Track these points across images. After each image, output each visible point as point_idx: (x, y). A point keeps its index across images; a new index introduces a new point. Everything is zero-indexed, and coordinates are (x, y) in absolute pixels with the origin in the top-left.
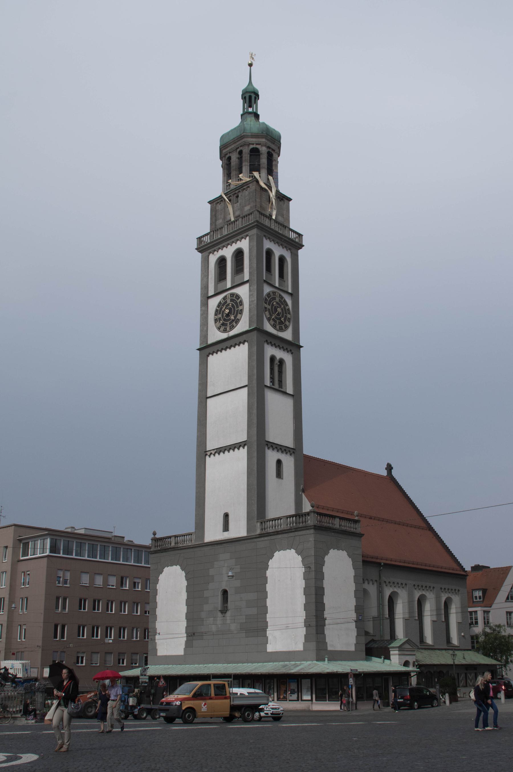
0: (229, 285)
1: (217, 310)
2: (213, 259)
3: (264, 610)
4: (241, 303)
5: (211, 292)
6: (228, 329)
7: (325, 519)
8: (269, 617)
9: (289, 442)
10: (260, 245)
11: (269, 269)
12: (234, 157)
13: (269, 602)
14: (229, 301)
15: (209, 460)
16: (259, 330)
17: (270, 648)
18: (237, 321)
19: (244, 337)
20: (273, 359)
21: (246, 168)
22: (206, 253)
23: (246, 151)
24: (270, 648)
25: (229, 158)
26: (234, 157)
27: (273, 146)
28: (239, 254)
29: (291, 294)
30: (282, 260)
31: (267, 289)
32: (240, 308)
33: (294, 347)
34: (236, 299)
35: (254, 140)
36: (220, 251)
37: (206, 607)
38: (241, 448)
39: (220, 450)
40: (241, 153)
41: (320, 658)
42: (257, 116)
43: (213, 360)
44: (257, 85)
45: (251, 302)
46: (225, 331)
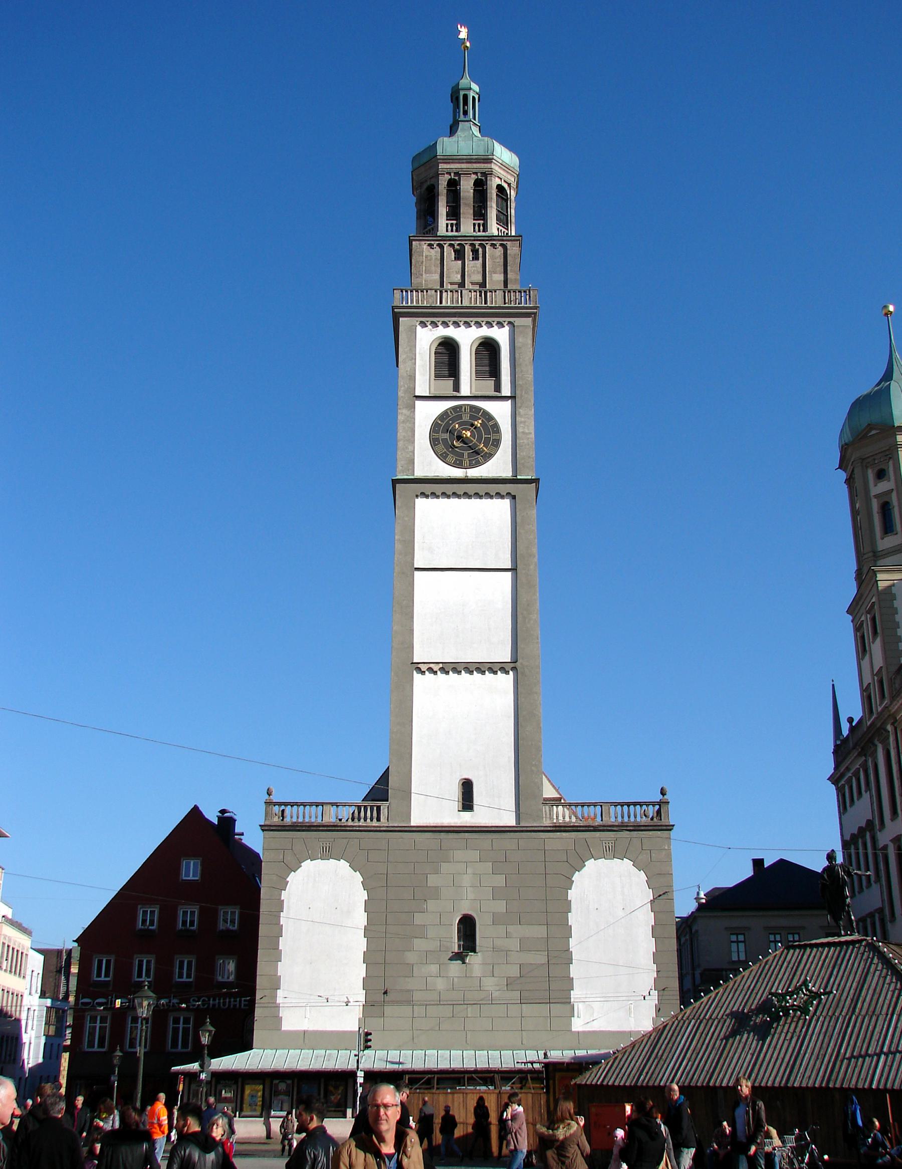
4: (496, 428)
6: (466, 462)
12: (467, 187)
17: (578, 1025)
18: (488, 456)
24: (578, 1025)
26: (467, 187)
32: (495, 436)
37: (419, 944)
39: (449, 668)
46: (458, 464)
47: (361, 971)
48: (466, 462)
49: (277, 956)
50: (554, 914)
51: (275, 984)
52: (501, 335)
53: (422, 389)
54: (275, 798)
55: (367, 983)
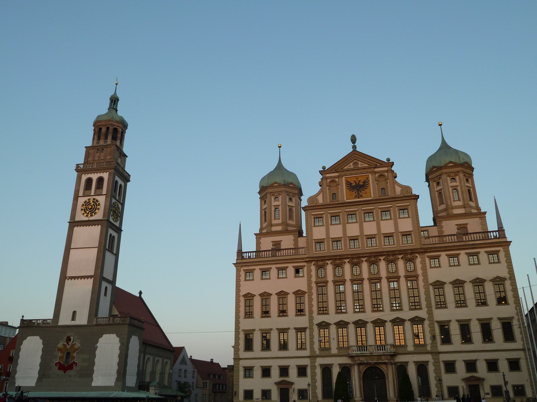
0: (93, 193)
1: (83, 205)
2: (84, 177)
3: (94, 364)
5: (81, 194)
6: (89, 216)
7: (133, 321)
8: (95, 368)
9: (110, 278)
10: (114, 178)
11: (115, 191)
12: (104, 130)
13: (96, 360)
14: (91, 202)
15: (67, 282)
16: (108, 220)
17: (94, 384)
19: (99, 222)
20: (111, 235)
21: (110, 137)
22: (80, 173)
23: (111, 128)
24: (94, 384)
25: (101, 129)
26: (104, 130)
27: (124, 129)
28: (100, 180)
29: (122, 204)
30: (121, 185)
31: (114, 200)
32: (98, 207)
33: (119, 230)
34: (96, 202)
35: (116, 124)
36: (89, 174)
38: (89, 279)
40: (108, 128)
41: (123, 390)
42: (117, 111)
43: (77, 230)
44: (119, 95)
45: (105, 206)
46: (87, 216)
47: (38, 368)
48: (89, 216)
49: (17, 364)
50: (91, 351)
51: (15, 372)
52: (105, 176)
53: (81, 194)
54: (24, 318)
55: (39, 372)
